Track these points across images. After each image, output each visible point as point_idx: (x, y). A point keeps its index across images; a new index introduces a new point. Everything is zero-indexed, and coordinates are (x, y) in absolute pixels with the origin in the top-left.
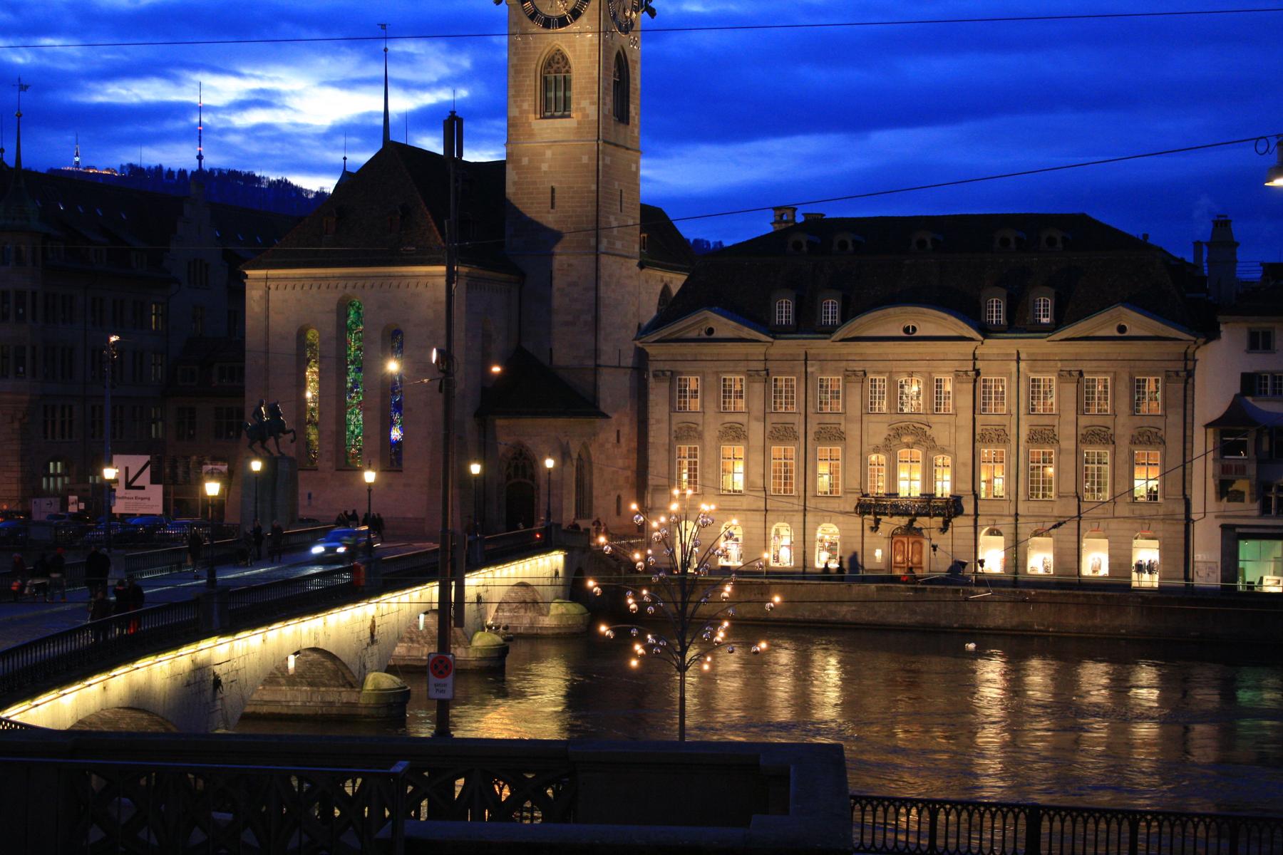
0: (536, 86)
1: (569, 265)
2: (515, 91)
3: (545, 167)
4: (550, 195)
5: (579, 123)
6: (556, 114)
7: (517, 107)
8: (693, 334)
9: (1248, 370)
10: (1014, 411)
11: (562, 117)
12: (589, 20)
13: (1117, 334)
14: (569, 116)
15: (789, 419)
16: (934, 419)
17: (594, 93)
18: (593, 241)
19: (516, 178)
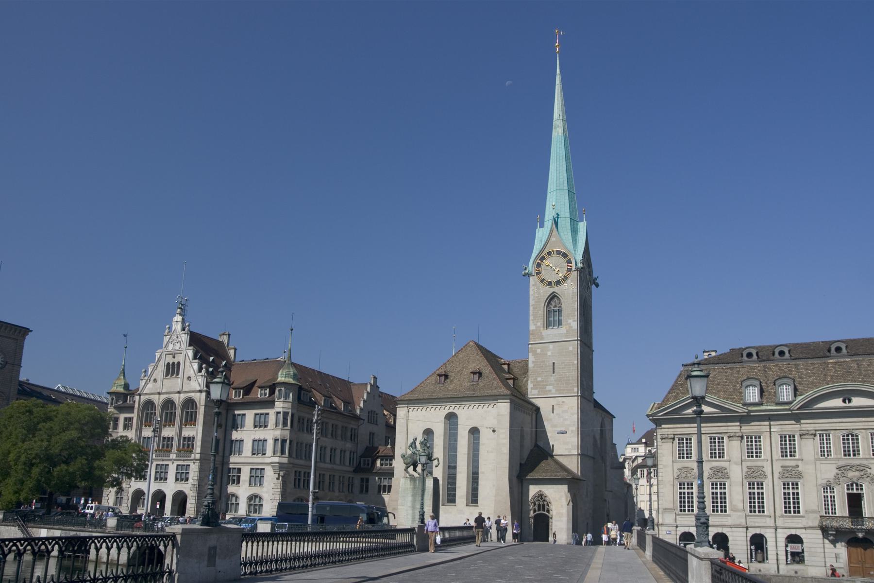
0: (544, 314)
1: (563, 402)
2: (533, 318)
3: (549, 353)
4: (552, 368)
7: (534, 325)
12: (572, 281)
15: (759, 464)
17: (575, 315)
18: (576, 389)
19: (534, 360)
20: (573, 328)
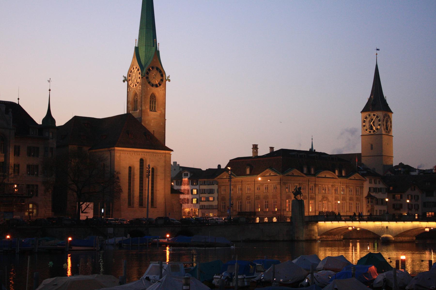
3: (152, 125)
5: (160, 114)
6: (153, 110)
8: (290, 174)
9: (370, 187)
10: (340, 194)
11: (154, 111)
12: (163, 86)
13: (354, 178)
14: (156, 111)
16: (329, 195)
20: (163, 113)
